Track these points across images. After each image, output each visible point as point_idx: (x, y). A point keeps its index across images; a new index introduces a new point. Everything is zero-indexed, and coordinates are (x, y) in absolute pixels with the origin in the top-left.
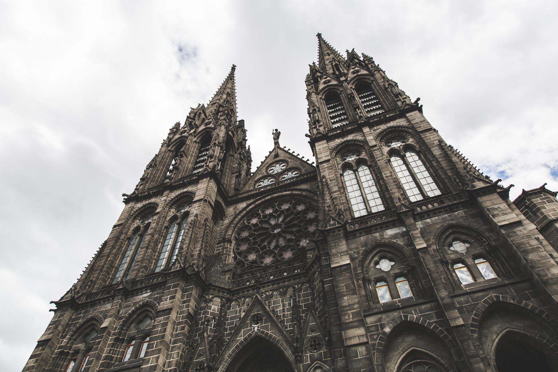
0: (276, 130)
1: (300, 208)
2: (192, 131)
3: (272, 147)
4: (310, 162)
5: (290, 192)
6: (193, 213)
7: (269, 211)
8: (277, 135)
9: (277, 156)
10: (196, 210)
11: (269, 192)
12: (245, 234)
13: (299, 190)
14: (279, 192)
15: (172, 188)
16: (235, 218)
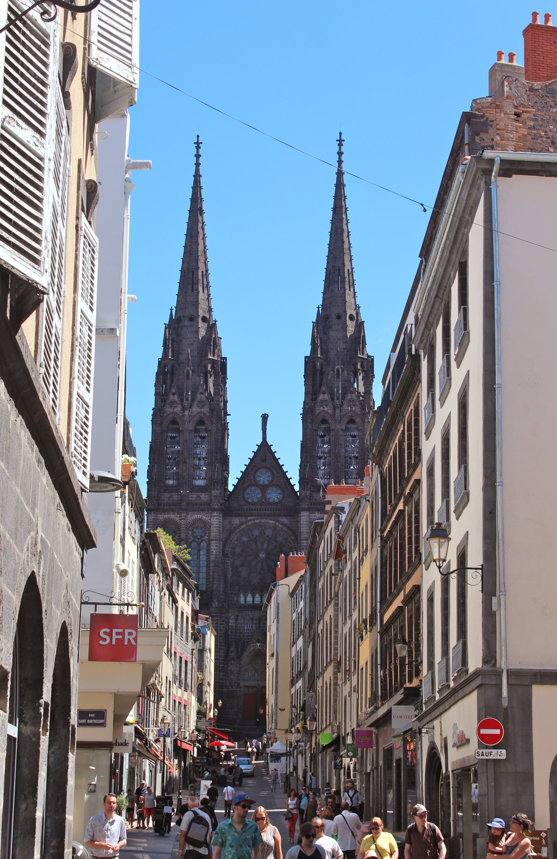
0: (266, 414)
1: (280, 539)
2: (186, 413)
3: (259, 441)
4: (292, 482)
5: (274, 522)
6: (213, 552)
7: (256, 533)
8: (265, 418)
9: (264, 461)
10: (215, 549)
11: (258, 516)
12: (238, 550)
13: (282, 524)
14: (266, 519)
15: (186, 510)
16: (230, 534)
